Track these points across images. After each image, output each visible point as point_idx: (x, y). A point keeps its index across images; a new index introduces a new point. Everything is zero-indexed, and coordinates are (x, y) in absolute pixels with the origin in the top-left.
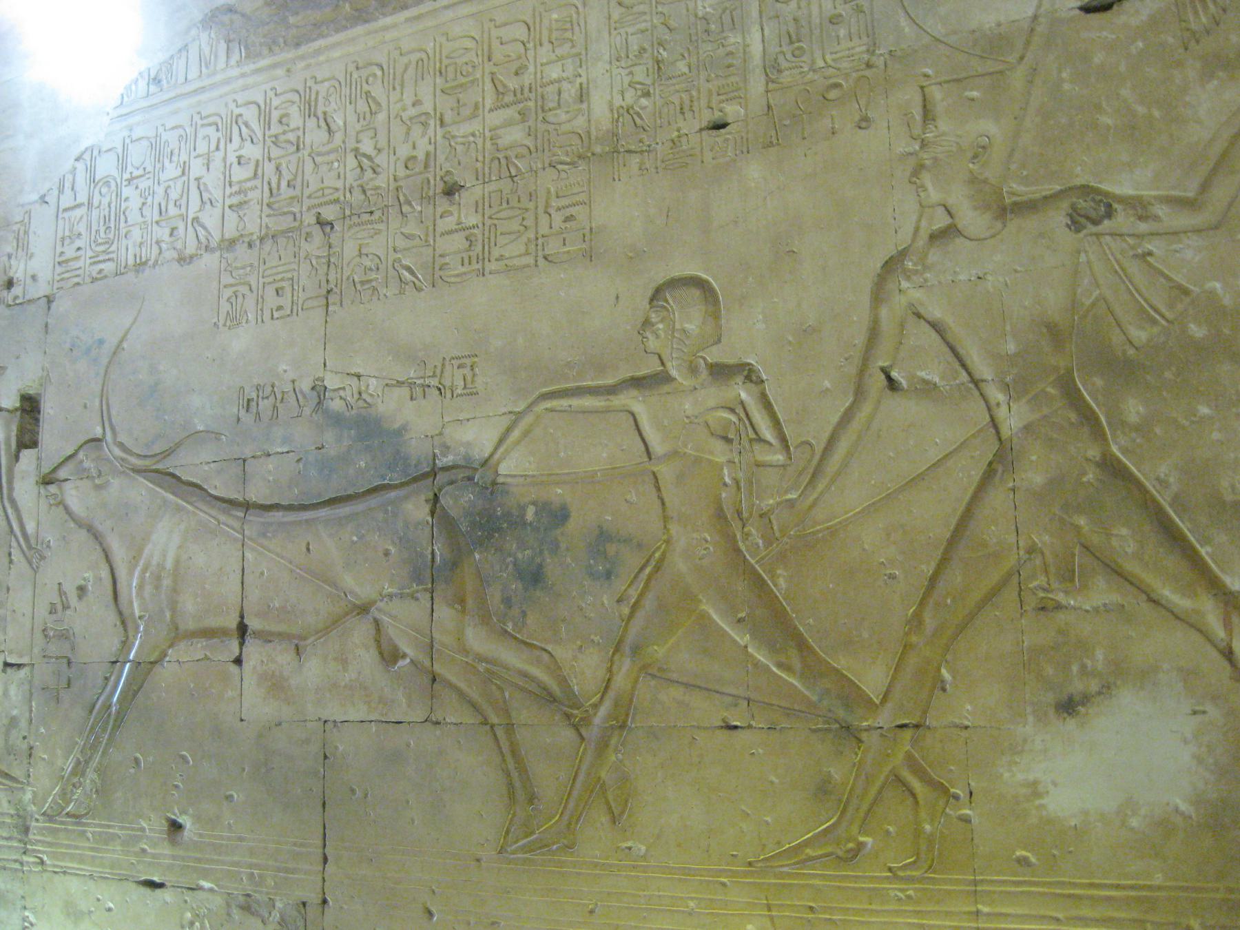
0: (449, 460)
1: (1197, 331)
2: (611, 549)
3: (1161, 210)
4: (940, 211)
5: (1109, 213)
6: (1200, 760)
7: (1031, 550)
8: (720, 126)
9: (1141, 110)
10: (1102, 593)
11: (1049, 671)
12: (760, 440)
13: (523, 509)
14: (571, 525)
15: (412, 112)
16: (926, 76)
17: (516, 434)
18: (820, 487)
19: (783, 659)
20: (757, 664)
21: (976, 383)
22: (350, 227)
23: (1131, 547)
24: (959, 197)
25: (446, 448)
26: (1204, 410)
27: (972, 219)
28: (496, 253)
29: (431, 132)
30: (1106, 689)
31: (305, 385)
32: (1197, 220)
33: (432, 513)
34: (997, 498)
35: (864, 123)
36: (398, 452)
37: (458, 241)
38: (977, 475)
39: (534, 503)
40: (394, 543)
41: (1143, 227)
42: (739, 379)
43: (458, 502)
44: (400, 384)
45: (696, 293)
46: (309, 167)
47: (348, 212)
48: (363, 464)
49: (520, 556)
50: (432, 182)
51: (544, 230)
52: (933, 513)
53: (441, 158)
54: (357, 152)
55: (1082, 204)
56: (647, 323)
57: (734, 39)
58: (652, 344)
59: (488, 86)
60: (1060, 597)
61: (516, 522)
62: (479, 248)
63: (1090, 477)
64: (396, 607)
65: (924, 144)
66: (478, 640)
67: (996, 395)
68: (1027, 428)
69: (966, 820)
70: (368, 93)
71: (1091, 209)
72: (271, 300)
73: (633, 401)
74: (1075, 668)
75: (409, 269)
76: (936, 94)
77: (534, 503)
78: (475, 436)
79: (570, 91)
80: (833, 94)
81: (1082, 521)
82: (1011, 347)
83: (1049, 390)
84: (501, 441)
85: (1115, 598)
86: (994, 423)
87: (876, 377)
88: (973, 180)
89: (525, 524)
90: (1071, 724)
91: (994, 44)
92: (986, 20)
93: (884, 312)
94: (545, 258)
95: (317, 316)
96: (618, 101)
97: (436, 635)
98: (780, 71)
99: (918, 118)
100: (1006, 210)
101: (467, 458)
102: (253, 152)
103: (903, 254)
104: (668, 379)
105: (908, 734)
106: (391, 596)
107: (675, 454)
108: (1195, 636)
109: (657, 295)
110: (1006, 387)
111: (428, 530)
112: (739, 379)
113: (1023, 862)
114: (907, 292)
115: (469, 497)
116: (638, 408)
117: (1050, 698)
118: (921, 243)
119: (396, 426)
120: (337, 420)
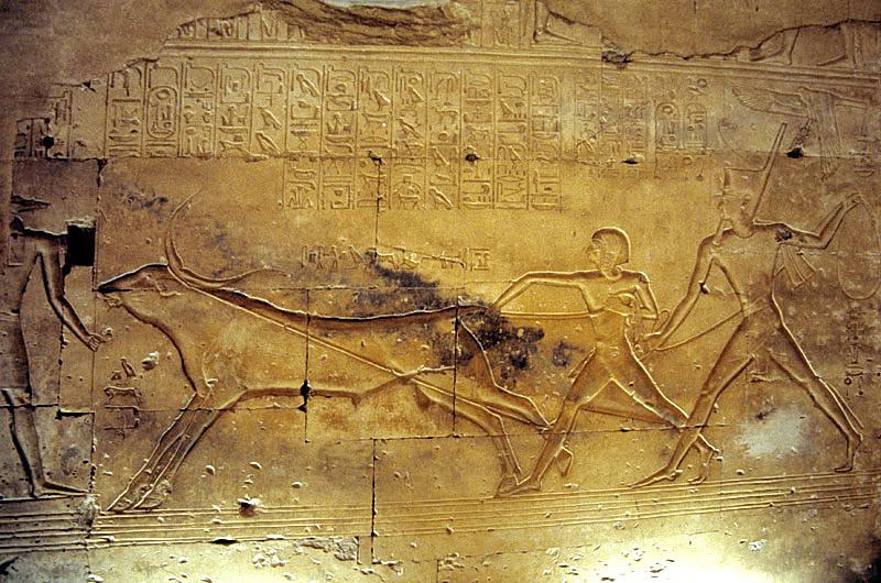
0: (468, 302)
1: (815, 285)
2: (567, 352)
3: (807, 238)
4: (729, 223)
5: (790, 237)
6: (801, 433)
7: (751, 360)
8: (631, 162)
9: (805, 199)
10: (775, 376)
11: (754, 403)
12: (645, 308)
13: (516, 330)
14: (544, 340)
15: (445, 108)
16: (727, 165)
17: (513, 293)
18: (672, 329)
19: (649, 401)
20: (638, 404)
21: (738, 294)
22: (395, 165)
23: (786, 360)
24: (736, 217)
25: (466, 296)
26: (814, 313)
27: (739, 228)
28: (502, 197)
29: (457, 122)
30: (773, 410)
31: (360, 251)
32: (820, 244)
33: (456, 329)
34: (741, 339)
35: (700, 178)
36: (433, 295)
37: (477, 187)
38: (734, 329)
39: (524, 328)
40: (428, 344)
41: (801, 243)
42: (637, 280)
43: (472, 326)
44: (434, 258)
45: (617, 238)
46: (362, 121)
47: (394, 155)
48: (406, 300)
49: (513, 353)
50: (458, 151)
51: (533, 190)
52: (716, 343)
53: (464, 139)
54: (402, 123)
55: (782, 231)
56: (591, 248)
57: (642, 123)
58: (594, 258)
59: (498, 107)
60: (760, 377)
61: (511, 336)
62: (490, 193)
63: (775, 333)
64: (428, 378)
65: (724, 193)
66: (487, 397)
67: (745, 300)
68: (755, 313)
69: (720, 460)
70: (411, 91)
71: (785, 236)
72: (330, 194)
73: (581, 283)
74: (764, 403)
75: (439, 195)
76: (731, 173)
77: (524, 328)
78: (488, 292)
79: (549, 125)
80: (687, 162)
81: (770, 349)
82: (751, 282)
83: (765, 300)
84: (502, 296)
85: (779, 378)
86: (742, 311)
87: (696, 286)
88: (742, 212)
89: (518, 338)
90: (761, 422)
91: (755, 159)
92: (755, 149)
93: (702, 260)
94: (533, 206)
95: (371, 212)
96: (578, 137)
97: (457, 392)
98: (663, 145)
99: (723, 181)
100: (753, 228)
101: (481, 303)
102: (316, 103)
103: (712, 238)
104: (601, 276)
105: (699, 429)
106: (426, 372)
107: (602, 310)
108: (805, 392)
109: (597, 235)
110: (748, 297)
111: (453, 338)
112: (637, 280)
113: (740, 474)
114: (712, 253)
115: (480, 323)
116: (582, 286)
117: (754, 414)
118: (720, 233)
119: (431, 281)
120: (387, 274)
